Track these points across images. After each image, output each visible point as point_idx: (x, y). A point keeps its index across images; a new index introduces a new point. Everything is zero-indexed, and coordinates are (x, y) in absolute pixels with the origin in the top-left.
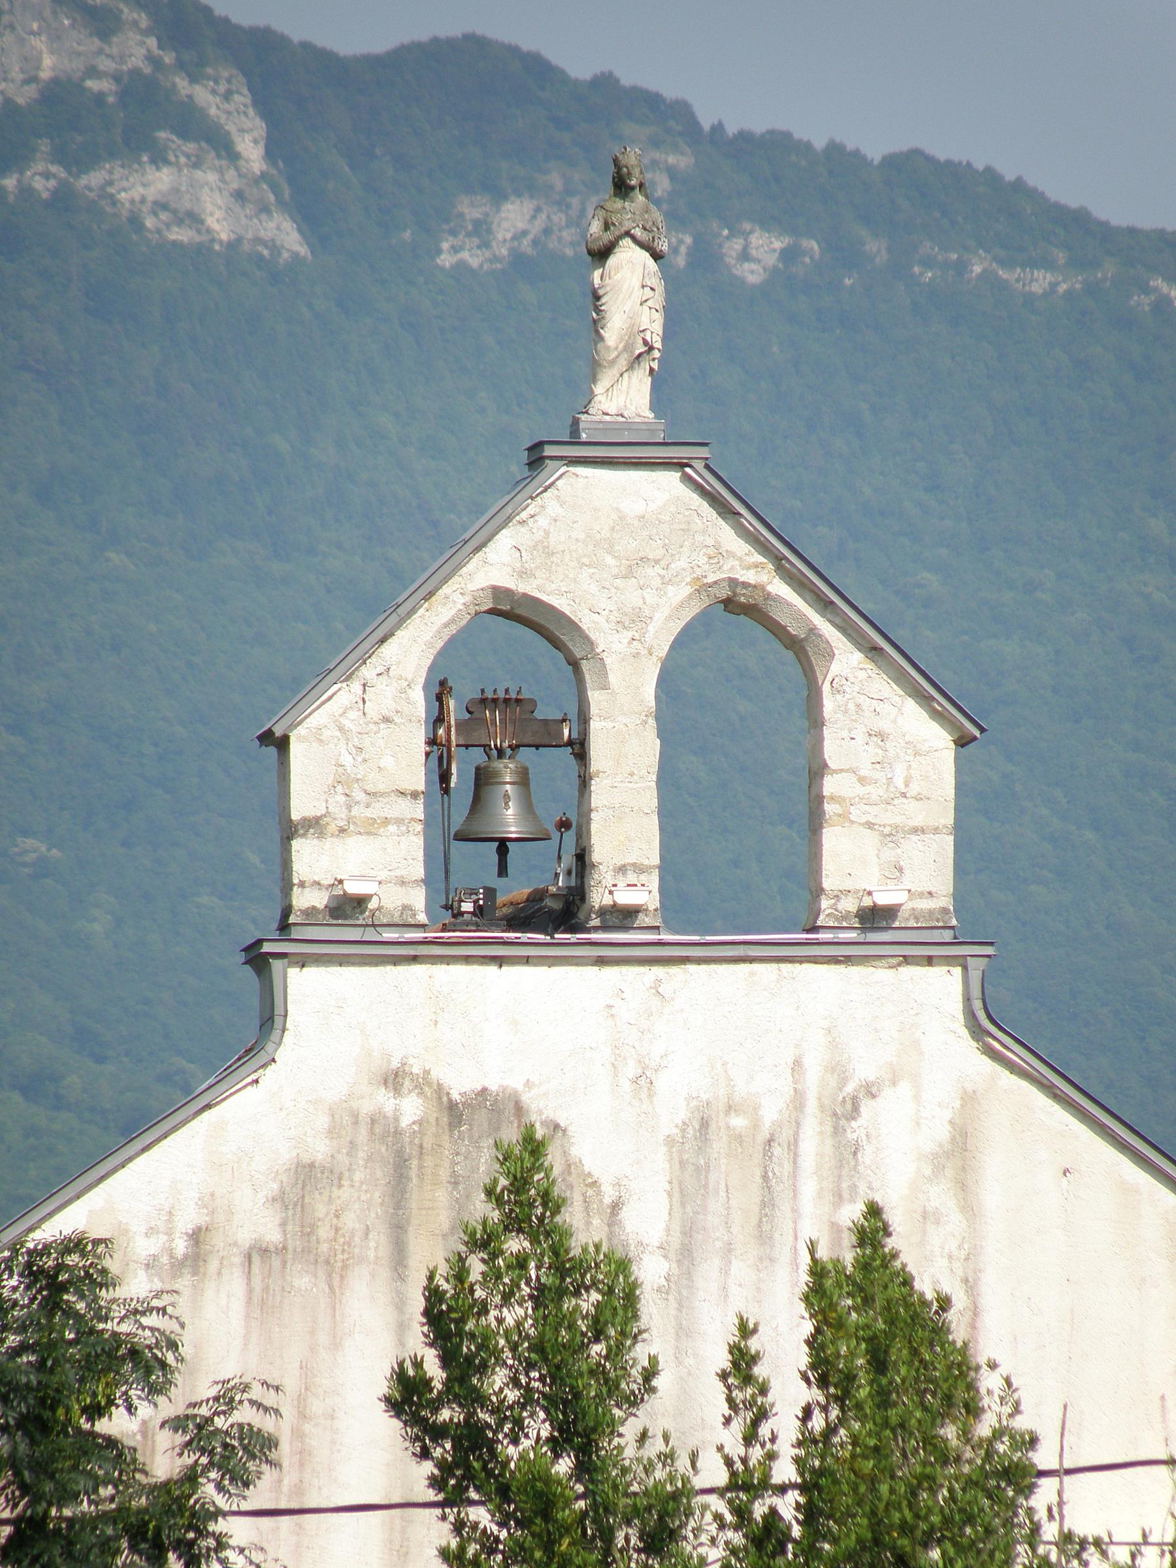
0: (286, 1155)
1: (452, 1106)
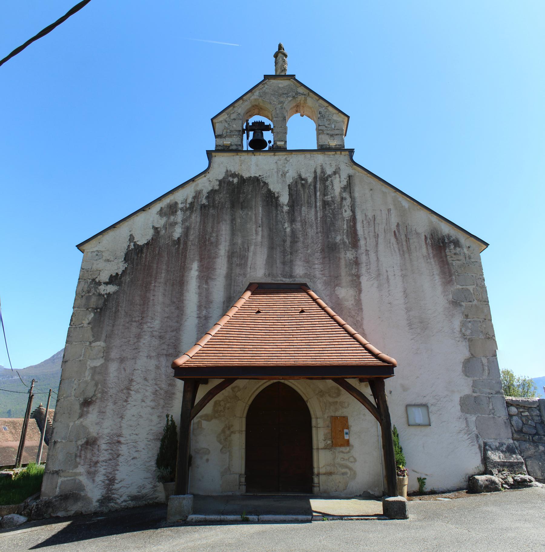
0: (210, 188)
1: (244, 179)
